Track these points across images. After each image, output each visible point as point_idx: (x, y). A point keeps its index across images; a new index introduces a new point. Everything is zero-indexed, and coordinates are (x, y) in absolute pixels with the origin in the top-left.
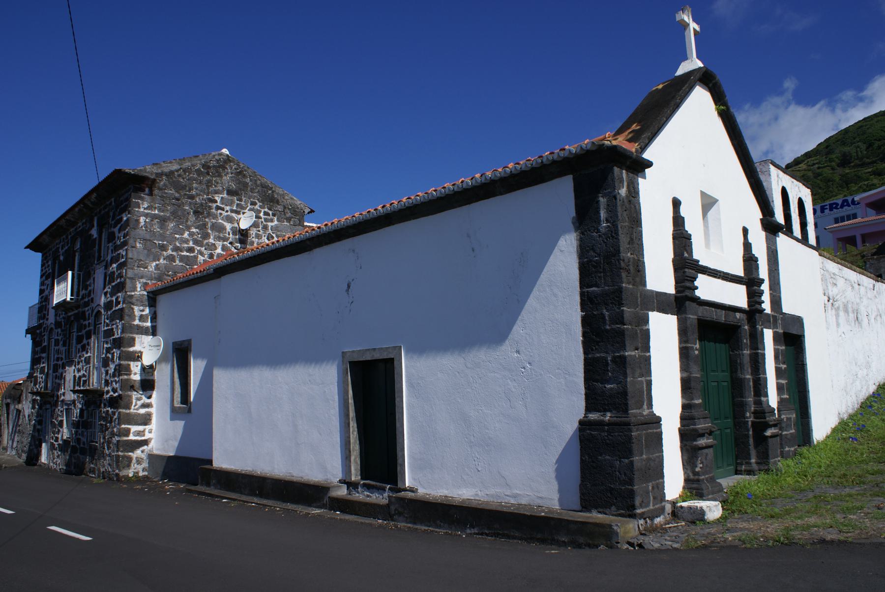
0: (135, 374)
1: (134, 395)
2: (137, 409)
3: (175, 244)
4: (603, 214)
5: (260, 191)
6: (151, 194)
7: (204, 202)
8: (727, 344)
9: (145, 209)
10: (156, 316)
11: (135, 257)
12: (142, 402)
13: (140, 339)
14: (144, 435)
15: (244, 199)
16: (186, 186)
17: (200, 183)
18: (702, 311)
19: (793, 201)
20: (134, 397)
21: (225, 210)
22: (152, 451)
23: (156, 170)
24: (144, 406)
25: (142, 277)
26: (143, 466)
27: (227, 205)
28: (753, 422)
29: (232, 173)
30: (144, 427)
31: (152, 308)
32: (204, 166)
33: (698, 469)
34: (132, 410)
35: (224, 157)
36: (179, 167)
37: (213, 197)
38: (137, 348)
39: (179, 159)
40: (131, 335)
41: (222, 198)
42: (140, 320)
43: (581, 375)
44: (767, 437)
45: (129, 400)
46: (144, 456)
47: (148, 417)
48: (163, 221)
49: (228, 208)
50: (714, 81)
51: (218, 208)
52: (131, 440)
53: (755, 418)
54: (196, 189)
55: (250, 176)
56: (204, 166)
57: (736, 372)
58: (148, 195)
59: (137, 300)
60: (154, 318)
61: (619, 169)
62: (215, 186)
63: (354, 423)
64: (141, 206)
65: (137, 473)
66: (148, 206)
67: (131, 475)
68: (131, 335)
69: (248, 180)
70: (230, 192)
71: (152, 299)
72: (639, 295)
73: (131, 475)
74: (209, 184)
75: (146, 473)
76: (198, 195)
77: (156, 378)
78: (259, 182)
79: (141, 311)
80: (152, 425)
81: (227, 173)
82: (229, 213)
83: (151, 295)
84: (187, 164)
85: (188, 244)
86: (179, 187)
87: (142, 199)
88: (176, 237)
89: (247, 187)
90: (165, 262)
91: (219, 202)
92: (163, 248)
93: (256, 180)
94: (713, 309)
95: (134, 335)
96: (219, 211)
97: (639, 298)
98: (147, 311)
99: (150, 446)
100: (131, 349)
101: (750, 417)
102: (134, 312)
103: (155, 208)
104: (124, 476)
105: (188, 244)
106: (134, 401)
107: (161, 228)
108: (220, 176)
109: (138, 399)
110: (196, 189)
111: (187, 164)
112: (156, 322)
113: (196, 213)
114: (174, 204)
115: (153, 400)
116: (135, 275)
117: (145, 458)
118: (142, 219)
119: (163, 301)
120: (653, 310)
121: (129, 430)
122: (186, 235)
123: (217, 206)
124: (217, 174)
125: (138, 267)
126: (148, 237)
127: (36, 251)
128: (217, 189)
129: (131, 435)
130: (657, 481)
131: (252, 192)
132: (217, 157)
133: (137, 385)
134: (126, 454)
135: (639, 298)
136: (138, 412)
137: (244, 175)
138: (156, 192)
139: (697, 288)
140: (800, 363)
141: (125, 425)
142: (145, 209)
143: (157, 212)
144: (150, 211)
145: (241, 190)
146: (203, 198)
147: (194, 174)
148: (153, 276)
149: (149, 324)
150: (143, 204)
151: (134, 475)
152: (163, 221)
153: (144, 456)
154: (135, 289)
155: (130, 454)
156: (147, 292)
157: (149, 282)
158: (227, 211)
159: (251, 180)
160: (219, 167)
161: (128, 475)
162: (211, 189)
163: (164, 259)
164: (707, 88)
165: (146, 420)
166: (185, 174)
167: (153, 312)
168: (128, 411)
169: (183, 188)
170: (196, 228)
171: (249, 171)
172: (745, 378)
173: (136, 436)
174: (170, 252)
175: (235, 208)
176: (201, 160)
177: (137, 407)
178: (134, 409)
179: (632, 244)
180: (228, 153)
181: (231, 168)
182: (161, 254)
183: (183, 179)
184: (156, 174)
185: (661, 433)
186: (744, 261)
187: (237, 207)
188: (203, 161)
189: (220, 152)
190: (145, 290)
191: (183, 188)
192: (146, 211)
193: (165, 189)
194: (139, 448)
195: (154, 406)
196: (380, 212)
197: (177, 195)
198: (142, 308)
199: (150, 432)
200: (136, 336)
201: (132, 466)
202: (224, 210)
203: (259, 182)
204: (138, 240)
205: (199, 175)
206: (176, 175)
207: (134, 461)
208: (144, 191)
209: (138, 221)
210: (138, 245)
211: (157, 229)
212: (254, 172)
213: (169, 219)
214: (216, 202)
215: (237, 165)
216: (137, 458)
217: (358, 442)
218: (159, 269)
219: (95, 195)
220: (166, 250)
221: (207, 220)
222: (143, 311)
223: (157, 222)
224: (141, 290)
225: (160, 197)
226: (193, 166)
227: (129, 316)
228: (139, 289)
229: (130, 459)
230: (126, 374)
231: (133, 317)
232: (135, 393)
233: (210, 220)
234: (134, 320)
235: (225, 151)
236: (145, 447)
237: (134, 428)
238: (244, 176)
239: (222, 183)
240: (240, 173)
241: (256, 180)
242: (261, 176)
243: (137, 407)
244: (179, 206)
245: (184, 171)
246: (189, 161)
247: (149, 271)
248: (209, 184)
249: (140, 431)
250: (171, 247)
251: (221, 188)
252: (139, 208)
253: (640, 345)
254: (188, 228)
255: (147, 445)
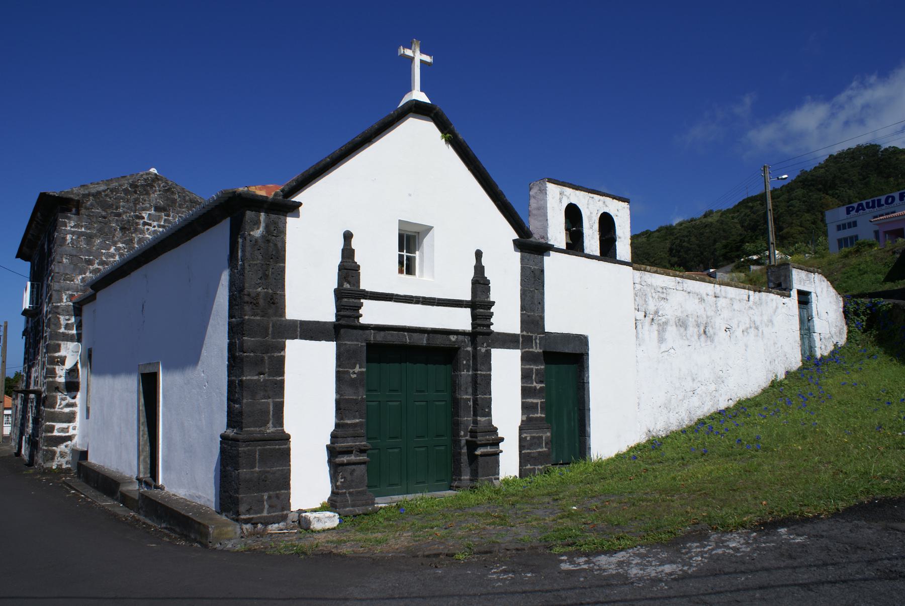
0: (60, 377)
1: (59, 396)
2: (62, 408)
3: (102, 259)
4: (240, 254)
5: (189, 206)
6: (78, 213)
7: (130, 219)
8: (448, 366)
9: (72, 227)
10: (81, 324)
11: (62, 271)
12: (66, 402)
13: (65, 346)
14: (68, 432)
15: (172, 214)
16: (113, 205)
17: (128, 201)
18: (372, 336)
19: (590, 218)
20: (59, 397)
21: (153, 225)
22: (76, 446)
23: (82, 191)
24: (68, 405)
25: (68, 290)
26: (66, 459)
27: (154, 221)
28: (467, 441)
29: (160, 191)
30: (68, 424)
31: (77, 317)
32: (131, 185)
33: (338, 483)
34: (56, 409)
35: (152, 176)
36: (106, 188)
37: (140, 214)
38: (62, 353)
39: (107, 180)
40: (57, 342)
41: (149, 214)
42: (66, 328)
43: (226, 395)
44: (477, 455)
45: (54, 400)
46: (67, 450)
47: (72, 416)
48: (89, 238)
49: (155, 223)
50: (435, 112)
51: (145, 224)
52: (55, 436)
53: (471, 437)
54: (123, 207)
55: (179, 193)
56: (131, 185)
57: (455, 392)
58: (75, 214)
59: (63, 310)
60: (79, 326)
61: (254, 212)
62: (143, 204)
63: (144, 427)
64: (68, 225)
65: (61, 465)
66: (75, 225)
67: (54, 467)
68: (57, 342)
69: (176, 196)
70: (157, 209)
71: (78, 310)
72: (271, 325)
73: (54, 467)
74: (136, 202)
75: (69, 466)
76: (125, 212)
77: (80, 380)
78: (187, 198)
79: (67, 320)
80: (76, 422)
81: (155, 191)
82: (156, 228)
83: (77, 306)
84: (114, 184)
85: (114, 258)
86: (105, 206)
87: (69, 218)
88: (102, 252)
89: (176, 203)
90: (91, 275)
91: (146, 218)
92: (90, 262)
93: (184, 197)
94: (406, 333)
95: (60, 342)
96: (147, 227)
97: (271, 328)
98: (73, 320)
99: (74, 441)
100: (57, 355)
101: (465, 435)
102: (60, 321)
103: (82, 226)
104: (47, 468)
105: (114, 258)
106: (59, 401)
107: (87, 244)
108: (148, 194)
109: (63, 399)
110: (123, 207)
111: (115, 184)
112: (81, 330)
113: (123, 229)
114: (100, 222)
115: (78, 400)
116: (61, 287)
117: (68, 452)
118: (69, 237)
119: (86, 309)
120: (293, 337)
121: (53, 427)
122: (112, 250)
123: (144, 222)
124: (144, 193)
125: (64, 280)
126: (74, 253)
127: (26, 260)
128: (144, 206)
129: (55, 431)
130: (278, 492)
131: (180, 208)
132: (145, 177)
133: (62, 387)
134: (50, 448)
135: (271, 328)
136: (63, 411)
137: (173, 192)
138: (83, 211)
139: (361, 316)
140: (582, 381)
141: (49, 422)
142: (72, 227)
143: (83, 230)
144: (76, 229)
145: (168, 205)
146: (130, 216)
147: (121, 194)
148: (79, 288)
149: (74, 332)
150: (69, 223)
151: (57, 467)
152: (89, 238)
153: (67, 450)
154: (61, 300)
155: (54, 448)
156: (73, 303)
157: (75, 293)
158: (154, 227)
159: (179, 197)
160: (147, 185)
161: (51, 468)
162: (138, 206)
163: (90, 273)
164: (429, 118)
165: (70, 418)
166: (112, 194)
167: (78, 321)
168: (52, 410)
169: (111, 206)
170: (122, 243)
171: (178, 188)
172: (461, 398)
173: (60, 432)
174: (96, 266)
175: (162, 223)
176: (129, 180)
177: (61, 406)
178: (58, 408)
179: (266, 279)
180: (156, 172)
181: (159, 186)
182: (87, 268)
183: (110, 198)
184: (83, 194)
185: (289, 449)
186: (472, 284)
187: (164, 222)
188: (130, 181)
189: (147, 172)
190: (71, 301)
191: (111, 206)
192: (72, 229)
193: (92, 209)
194: (62, 443)
195: (79, 405)
196: (149, 240)
197: (104, 213)
198: (67, 317)
199: (74, 429)
200: (62, 343)
201: (56, 459)
202: (151, 226)
203: (187, 198)
204: (65, 256)
205: (126, 194)
206: (103, 195)
207: (58, 454)
208: (70, 211)
209: (64, 239)
210: (64, 260)
211: (83, 245)
212: (183, 189)
213: (95, 235)
214: (143, 218)
215: (166, 183)
216: (60, 452)
217: (148, 444)
218: (85, 281)
219: (39, 214)
220: (92, 264)
221: (134, 235)
222: (69, 320)
223: (84, 239)
224: (67, 301)
225: (87, 216)
226: (121, 185)
227: (55, 324)
228: (65, 301)
229: (54, 453)
230: (51, 377)
231: (58, 325)
232: (60, 394)
233: (137, 235)
234: (60, 328)
235: (153, 170)
236: (69, 442)
237: (58, 426)
238: (173, 193)
239: (150, 201)
240: (169, 190)
241: (184, 197)
242: (189, 192)
243: (61, 406)
244: (106, 224)
245: (110, 191)
246: (116, 181)
247: (75, 284)
248: (137, 202)
249: (64, 428)
250: (98, 261)
251: (148, 205)
252: (66, 226)
253: (267, 370)
254: (115, 243)
255: (71, 441)
